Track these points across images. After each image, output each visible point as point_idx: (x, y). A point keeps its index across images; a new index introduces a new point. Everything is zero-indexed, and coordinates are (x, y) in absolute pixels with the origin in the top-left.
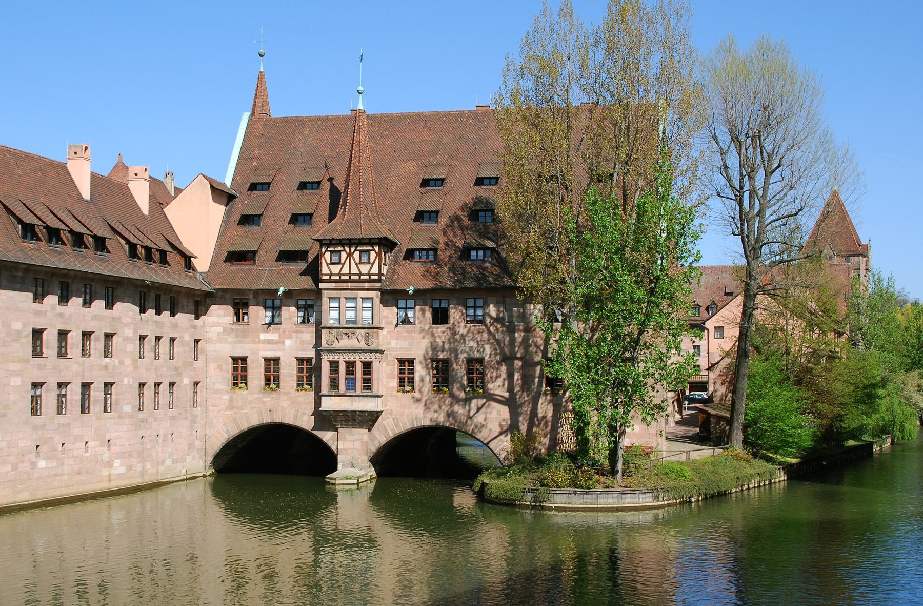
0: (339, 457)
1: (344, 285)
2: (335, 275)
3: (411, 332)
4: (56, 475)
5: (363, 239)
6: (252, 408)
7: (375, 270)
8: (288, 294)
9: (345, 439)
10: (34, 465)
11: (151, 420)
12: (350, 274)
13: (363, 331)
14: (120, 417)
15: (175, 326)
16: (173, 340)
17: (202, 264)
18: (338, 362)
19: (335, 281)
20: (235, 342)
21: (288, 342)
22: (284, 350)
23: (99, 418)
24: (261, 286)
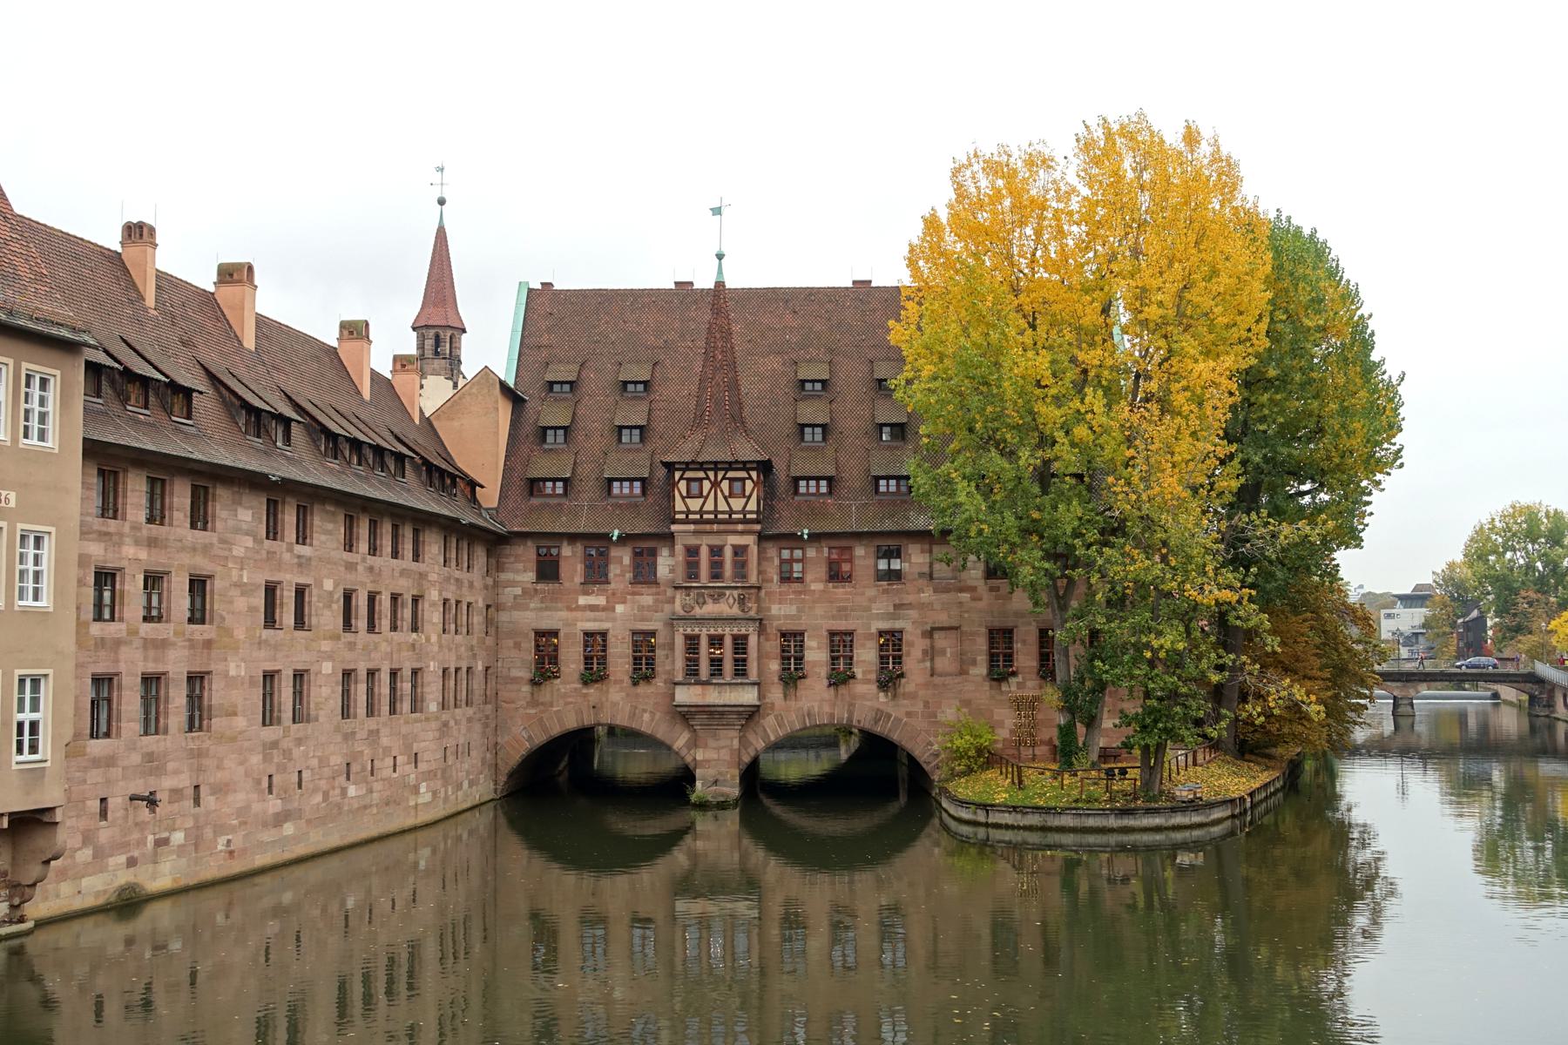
0: (698, 773)
1: (708, 527)
2: (695, 513)
3: (800, 593)
4: (365, 807)
5: (737, 462)
6: (567, 704)
7: (752, 506)
8: (624, 539)
9: (706, 746)
10: (344, 791)
11: (452, 723)
12: (716, 512)
13: (735, 593)
14: (427, 719)
15: (471, 585)
16: (469, 605)
17: (490, 495)
18: (698, 636)
19: (695, 522)
20: (541, 609)
21: (620, 608)
22: (614, 620)
23: (407, 722)
24: (581, 530)
